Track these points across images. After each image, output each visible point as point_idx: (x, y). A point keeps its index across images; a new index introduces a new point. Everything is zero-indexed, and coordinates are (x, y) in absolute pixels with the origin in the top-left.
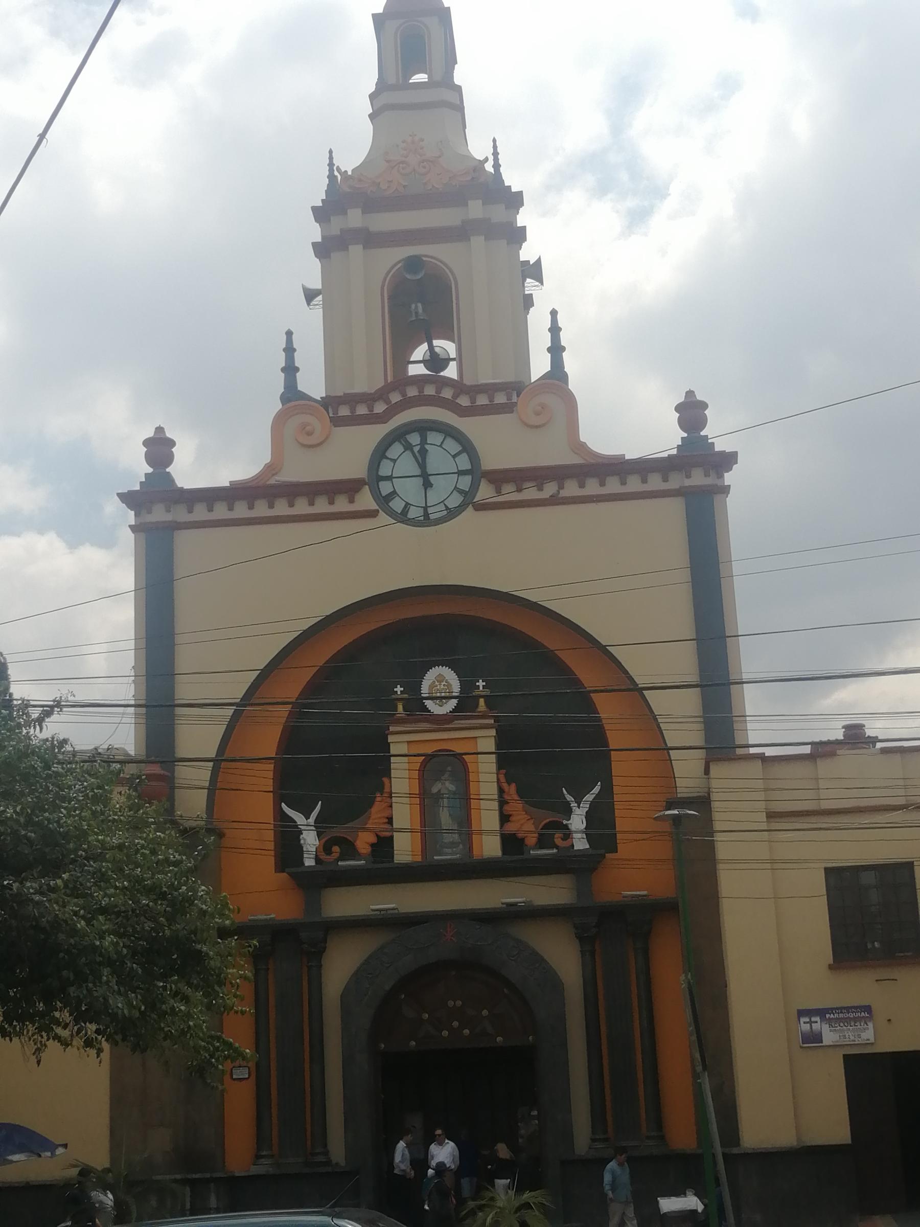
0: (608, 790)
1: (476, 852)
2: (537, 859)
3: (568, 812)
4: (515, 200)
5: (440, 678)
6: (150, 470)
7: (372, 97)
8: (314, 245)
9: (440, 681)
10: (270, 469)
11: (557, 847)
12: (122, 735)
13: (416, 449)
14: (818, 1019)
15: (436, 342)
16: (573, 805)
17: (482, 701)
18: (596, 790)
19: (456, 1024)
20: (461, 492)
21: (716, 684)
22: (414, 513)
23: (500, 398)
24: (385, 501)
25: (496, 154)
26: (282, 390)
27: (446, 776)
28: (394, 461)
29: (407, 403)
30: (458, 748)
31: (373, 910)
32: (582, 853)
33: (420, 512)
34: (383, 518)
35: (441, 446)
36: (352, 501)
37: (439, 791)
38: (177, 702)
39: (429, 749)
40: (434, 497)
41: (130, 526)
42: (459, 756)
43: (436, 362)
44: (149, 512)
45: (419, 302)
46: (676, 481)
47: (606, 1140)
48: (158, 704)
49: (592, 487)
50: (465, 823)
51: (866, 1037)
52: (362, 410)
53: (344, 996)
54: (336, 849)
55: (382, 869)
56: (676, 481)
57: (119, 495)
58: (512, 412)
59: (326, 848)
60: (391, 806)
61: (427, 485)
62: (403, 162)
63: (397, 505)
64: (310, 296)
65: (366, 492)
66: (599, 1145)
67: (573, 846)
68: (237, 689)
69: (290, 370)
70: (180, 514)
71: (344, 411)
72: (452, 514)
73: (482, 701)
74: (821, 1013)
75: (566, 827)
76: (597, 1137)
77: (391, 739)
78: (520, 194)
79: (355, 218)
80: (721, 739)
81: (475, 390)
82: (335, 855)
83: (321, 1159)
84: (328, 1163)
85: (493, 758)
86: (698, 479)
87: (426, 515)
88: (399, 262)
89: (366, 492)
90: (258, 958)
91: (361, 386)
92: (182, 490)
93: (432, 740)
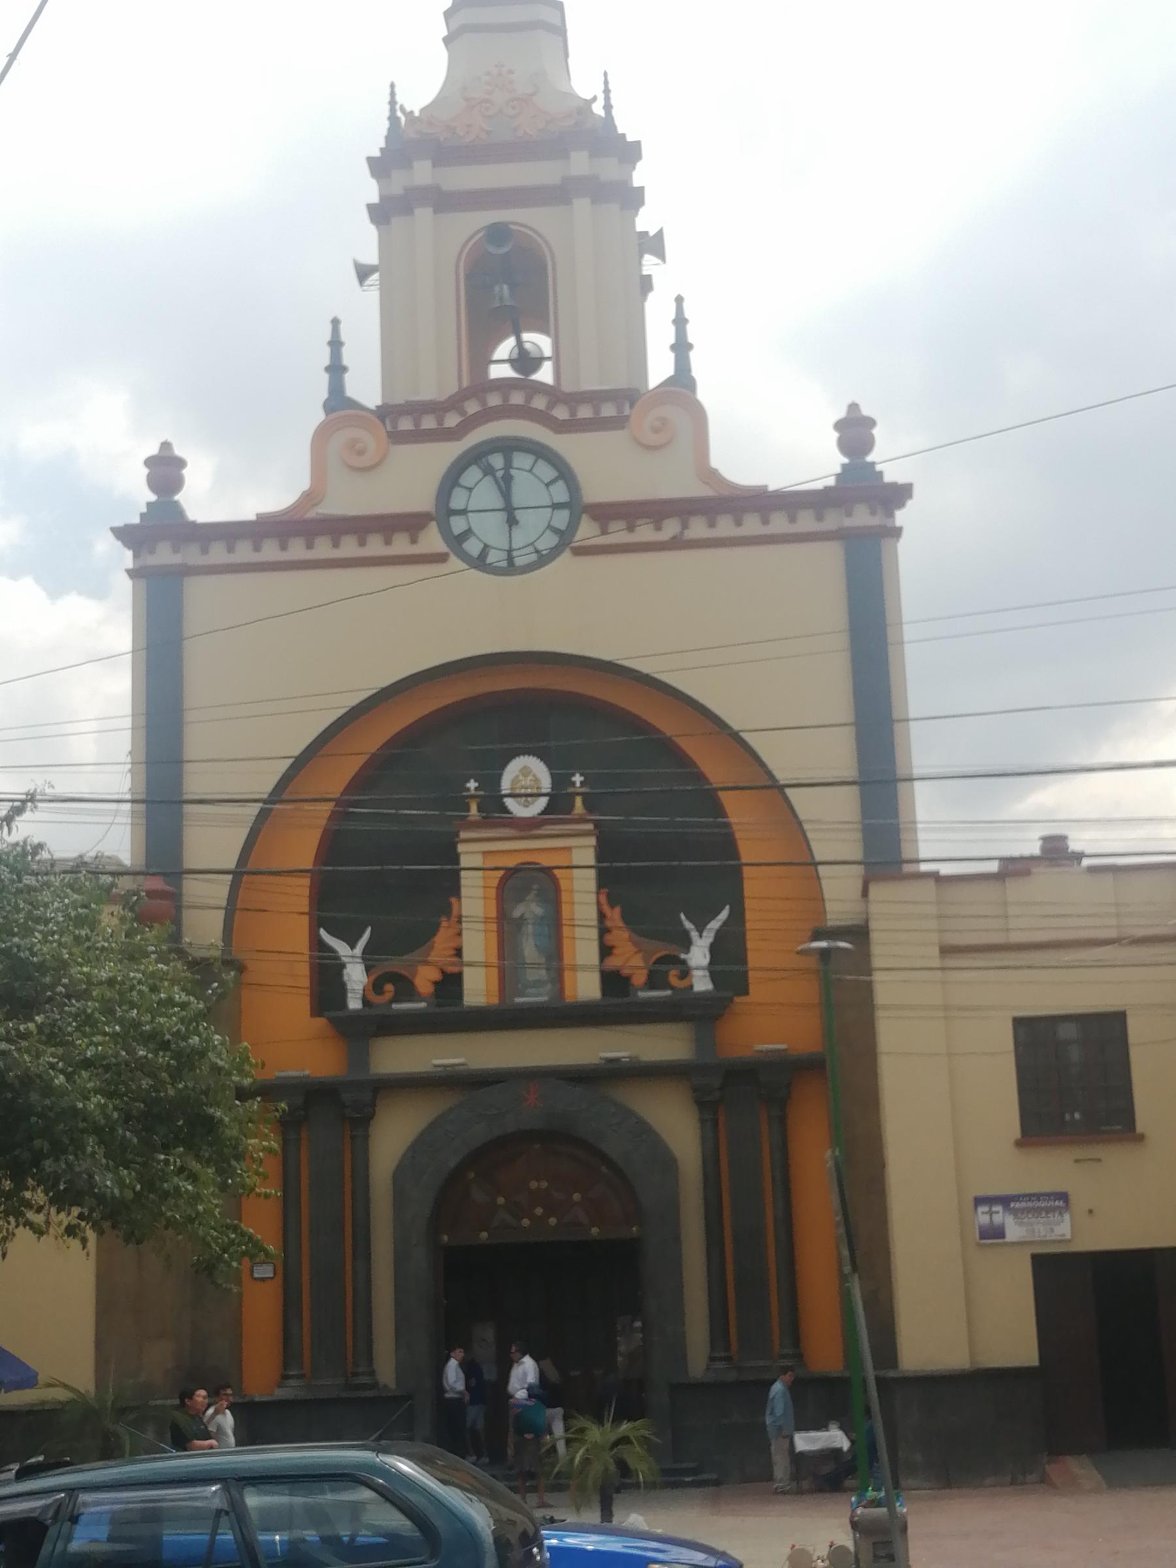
0: (738, 916)
1: (568, 992)
2: (650, 1003)
3: (687, 944)
4: (631, 153)
5: (526, 771)
6: (153, 498)
7: (448, 15)
8: (370, 207)
9: (526, 775)
10: (309, 498)
11: (672, 988)
12: (114, 839)
13: (500, 474)
14: (998, 1208)
15: (527, 336)
16: (694, 934)
17: (579, 801)
18: (724, 914)
19: (539, 1211)
20: (556, 531)
21: (879, 781)
22: (493, 557)
23: (608, 410)
24: (457, 542)
25: (607, 91)
26: (324, 395)
27: (531, 896)
28: (470, 490)
29: (488, 415)
30: (546, 861)
31: (436, 1066)
32: (703, 995)
33: (504, 555)
34: (455, 562)
35: (530, 471)
36: (414, 541)
38: (186, 797)
39: (511, 862)
40: (520, 538)
41: (128, 571)
42: (548, 871)
43: (525, 361)
44: (152, 552)
45: (504, 284)
46: (833, 521)
47: (729, 1359)
48: (162, 796)
49: (725, 527)
50: (555, 954)
51: (1061, 1232)
52: (429, 423)
53: (398, 1175)
54: (389, 987)
55: (448, 1013)
56: (833, 521)
57: (113, 530)
58: (623, 428)
59: (377, 986)
60: (460, 934)
61: (512, 521)
63: (473, 547)
64: (363, 273)
65: (433, 528)
66: (719, 1365)
67: (691, 987)
68: (264, 781)
69: (336, 369)
70: (192, 555)
71: (406, 424)
72: (543, 559)
73: (579, 801)
74: (1005, 1201)
75: (684, 962)
76: (717, 1355)
77: (461, 848)
78: (637, 144)
79: (423, 173)
80: (884, 852)
81: (574, 399)
82: (388, 996)
84: (374, 1386)
85: (592, 873)
86: (861, 517)
87: (510, 559)
88: (478, 232)
89: (433, 528)
90: (289, 1126)
91: (428, 392)
92: (194, 525)
93: (515, 850)
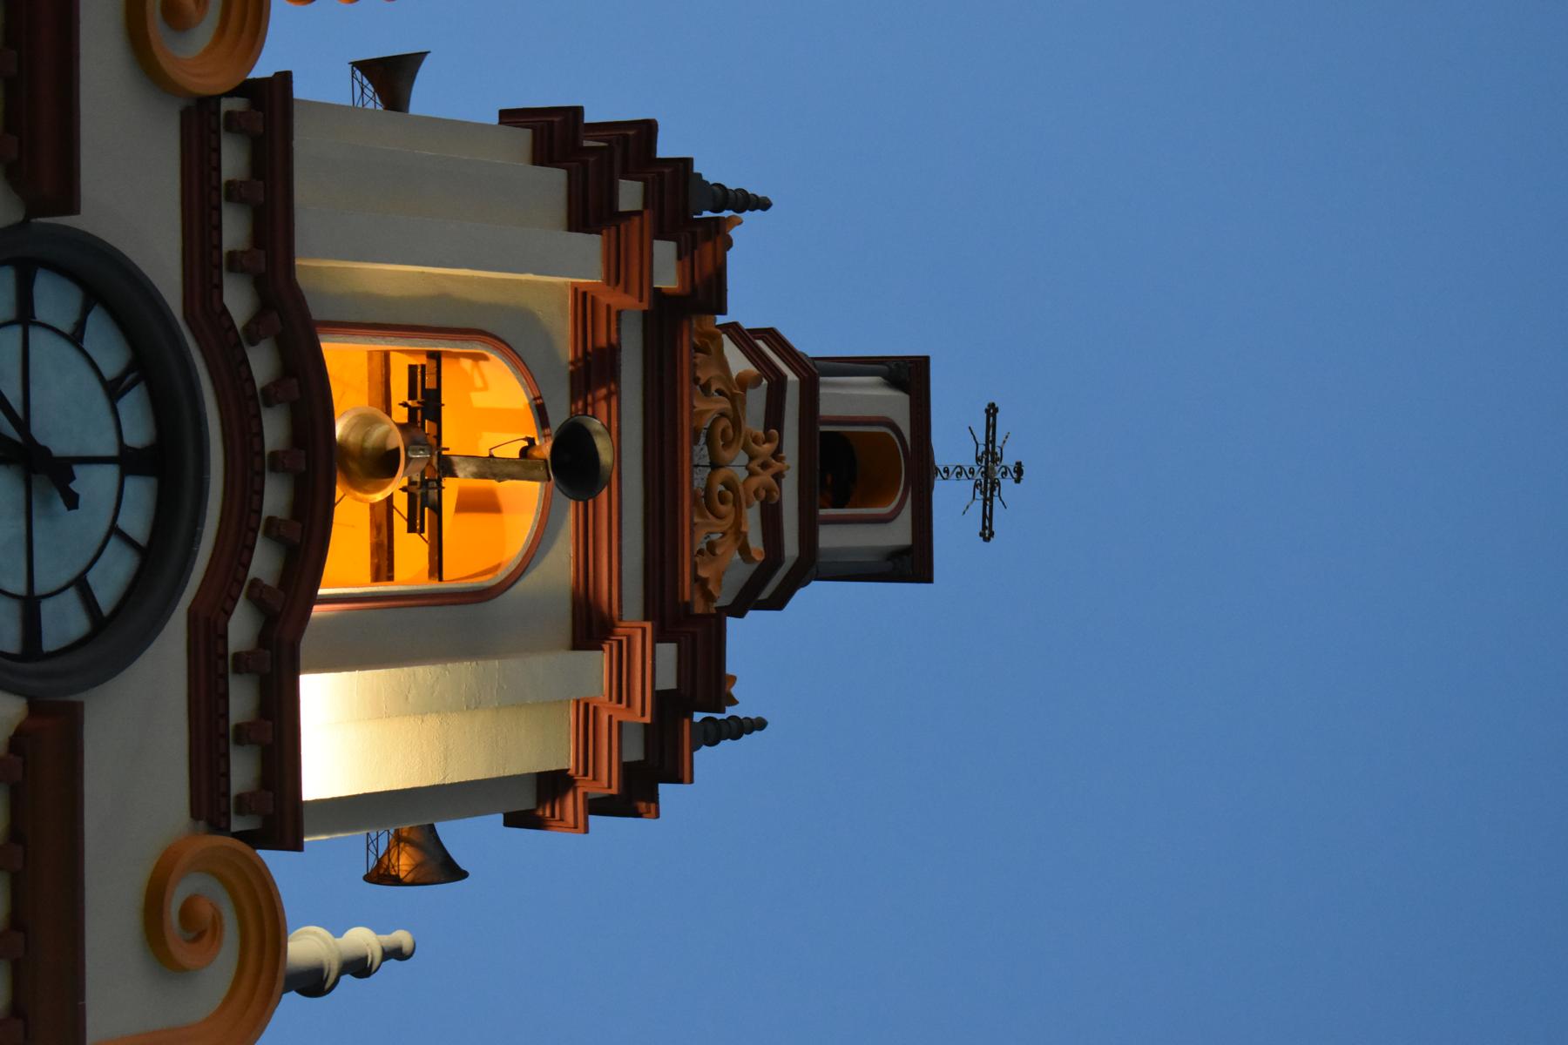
28: (76, 338)
35: (114, 530)
52: (234, 231)
58: (195, 813)
62: (737, 424)
64: (390, 77)
71: (233, 161)
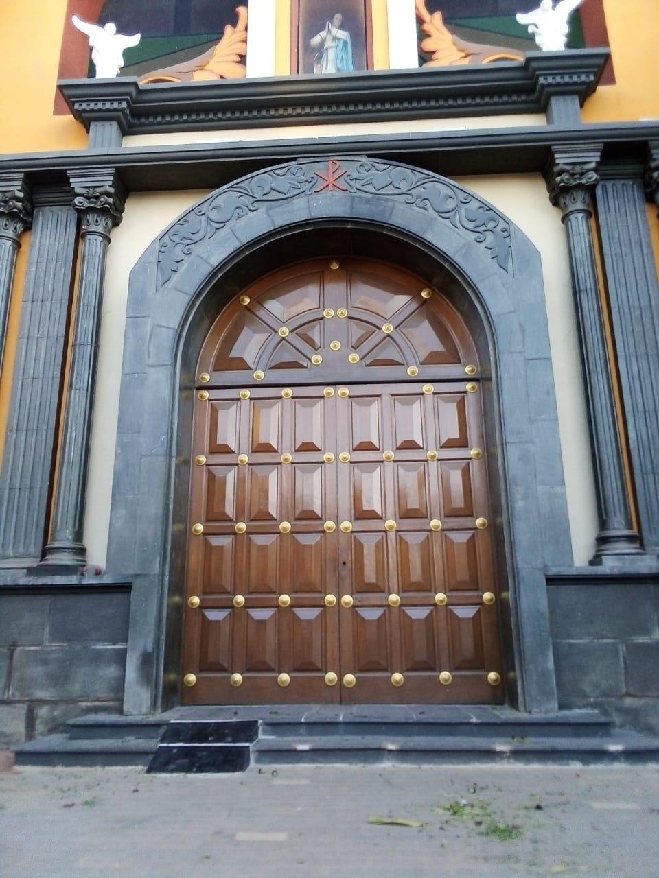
37: (323, 42)
53: (133, 275)
60: (245, 41)
83: (66, 559)
